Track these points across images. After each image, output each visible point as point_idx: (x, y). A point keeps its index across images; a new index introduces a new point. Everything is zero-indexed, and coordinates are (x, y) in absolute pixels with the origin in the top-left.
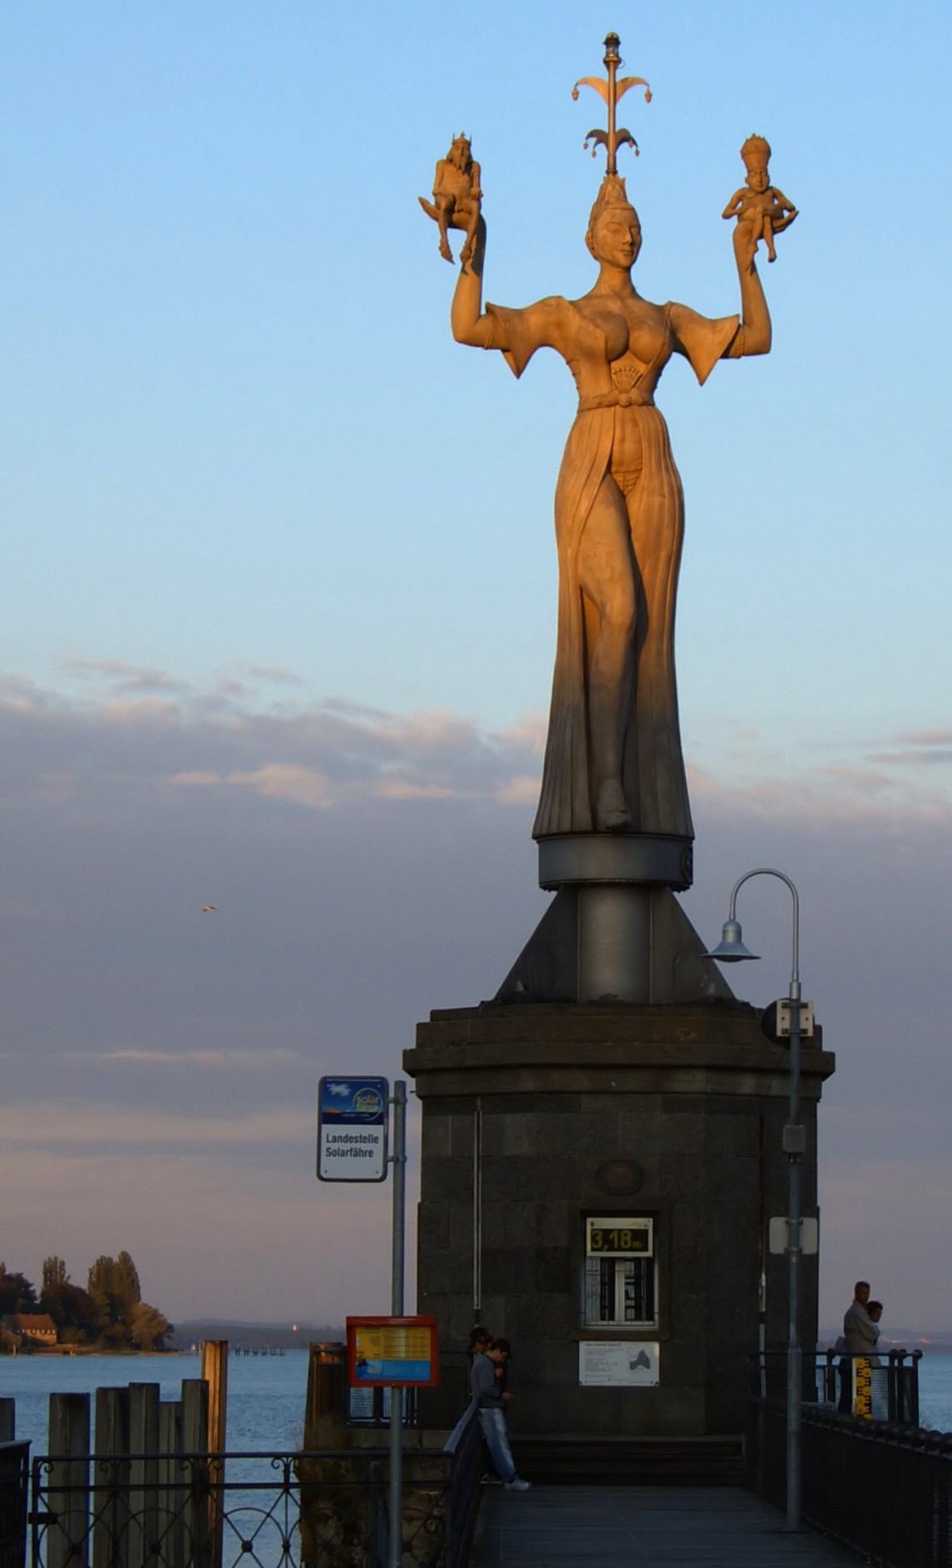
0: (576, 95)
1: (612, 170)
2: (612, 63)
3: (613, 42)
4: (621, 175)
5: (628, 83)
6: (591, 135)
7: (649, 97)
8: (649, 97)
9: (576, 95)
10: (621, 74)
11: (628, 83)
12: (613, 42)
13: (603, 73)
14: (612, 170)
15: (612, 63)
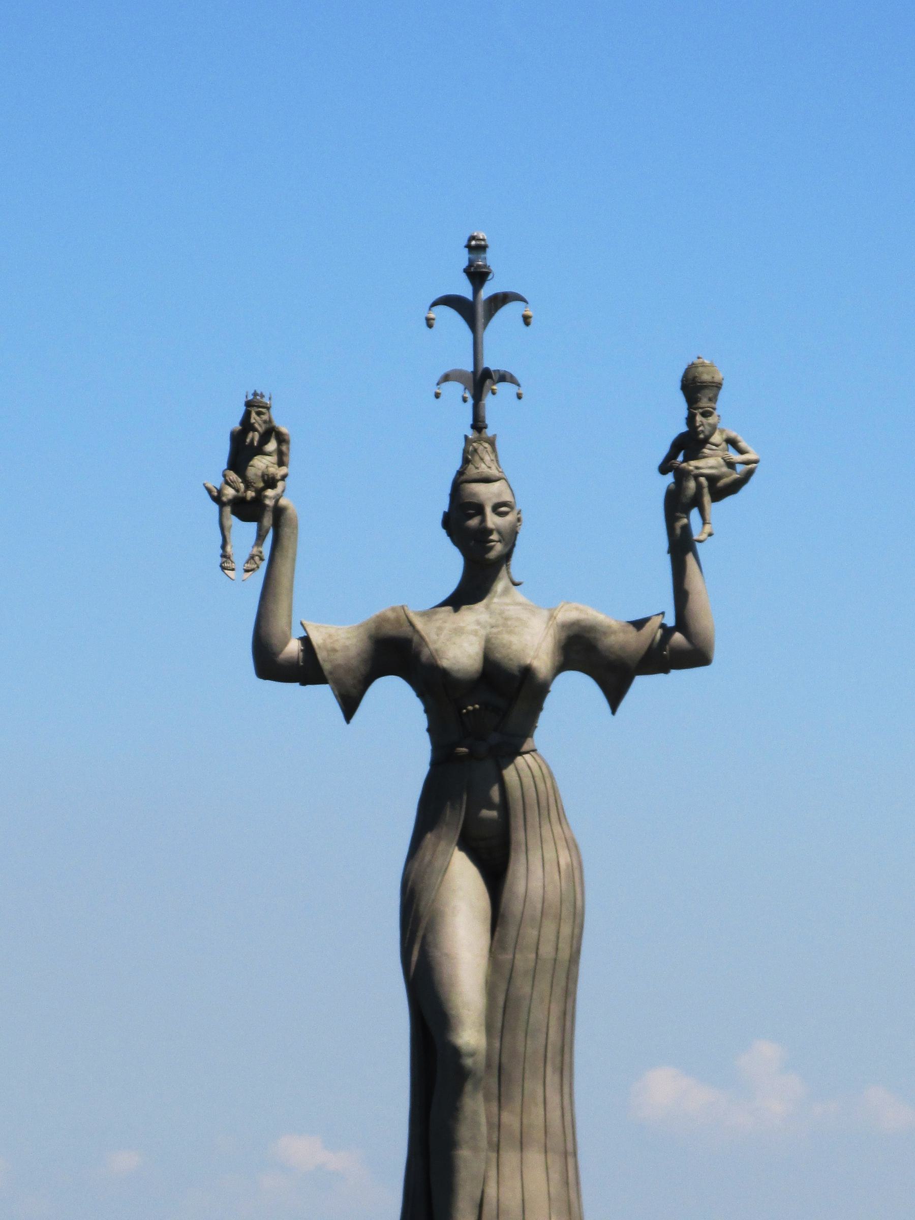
0: (429, 323)
1: (478, 425)
2: (477, 276)
3: (476, 247)
4: (489, 432)
5: (499, 301)
6: (446, 378)
7: (526, 320)
8: (526, 320)
9: (429, 323)
10: (486, 292)
11: (499, 301)
12: (476, 247)
13: (464, 289)
14: (478, 425)
15: (477, 276)
